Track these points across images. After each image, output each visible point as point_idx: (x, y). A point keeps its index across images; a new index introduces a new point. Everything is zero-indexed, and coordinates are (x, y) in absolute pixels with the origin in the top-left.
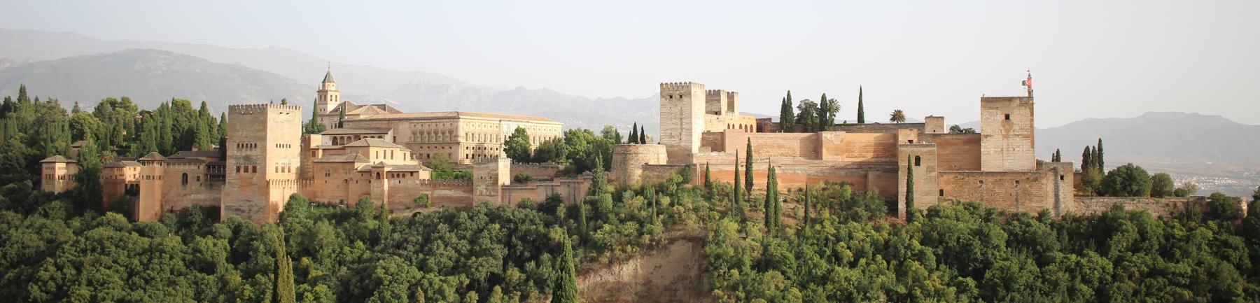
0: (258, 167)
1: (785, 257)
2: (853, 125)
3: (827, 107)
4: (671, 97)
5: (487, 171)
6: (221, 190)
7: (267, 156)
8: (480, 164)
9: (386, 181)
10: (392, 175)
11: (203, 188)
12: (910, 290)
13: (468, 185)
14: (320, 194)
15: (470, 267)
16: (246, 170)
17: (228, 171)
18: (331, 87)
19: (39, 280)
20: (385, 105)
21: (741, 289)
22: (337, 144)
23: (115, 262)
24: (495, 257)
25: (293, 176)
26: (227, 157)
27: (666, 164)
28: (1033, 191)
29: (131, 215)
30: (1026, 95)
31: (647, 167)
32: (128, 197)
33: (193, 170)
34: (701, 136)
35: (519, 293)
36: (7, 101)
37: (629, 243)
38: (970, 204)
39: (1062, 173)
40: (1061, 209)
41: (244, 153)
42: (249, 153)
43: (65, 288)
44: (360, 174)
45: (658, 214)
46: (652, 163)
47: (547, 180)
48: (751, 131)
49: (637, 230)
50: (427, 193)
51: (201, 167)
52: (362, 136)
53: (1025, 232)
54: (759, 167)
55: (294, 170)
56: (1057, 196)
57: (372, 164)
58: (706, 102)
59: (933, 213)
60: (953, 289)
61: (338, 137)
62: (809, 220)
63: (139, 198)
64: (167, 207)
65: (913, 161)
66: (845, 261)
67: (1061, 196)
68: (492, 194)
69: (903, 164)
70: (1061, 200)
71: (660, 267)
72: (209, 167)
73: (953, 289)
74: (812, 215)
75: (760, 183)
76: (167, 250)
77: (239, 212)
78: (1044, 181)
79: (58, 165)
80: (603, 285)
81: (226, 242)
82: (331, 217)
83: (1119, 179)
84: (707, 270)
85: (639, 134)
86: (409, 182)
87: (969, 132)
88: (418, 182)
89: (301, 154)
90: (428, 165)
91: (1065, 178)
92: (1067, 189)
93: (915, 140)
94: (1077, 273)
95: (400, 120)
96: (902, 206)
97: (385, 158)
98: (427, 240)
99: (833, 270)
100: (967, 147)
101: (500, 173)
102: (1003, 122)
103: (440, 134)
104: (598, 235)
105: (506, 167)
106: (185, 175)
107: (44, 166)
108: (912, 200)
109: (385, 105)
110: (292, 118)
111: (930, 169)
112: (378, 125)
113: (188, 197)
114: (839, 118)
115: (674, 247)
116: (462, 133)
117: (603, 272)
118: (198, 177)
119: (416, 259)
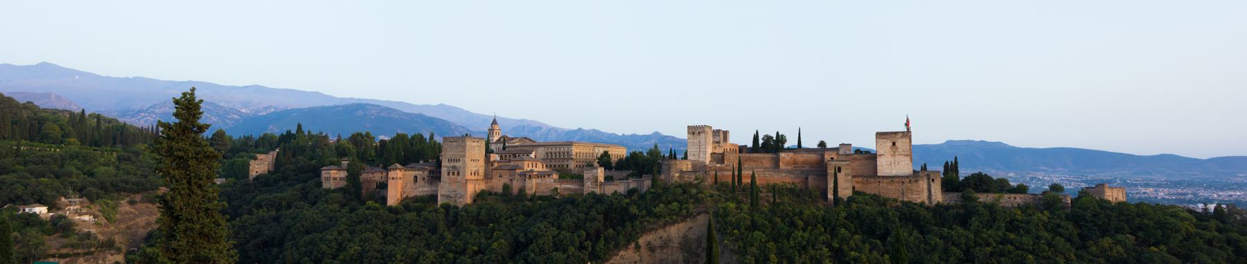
3: (781, 139)
5: (591, 174)
16: (453, 174)
29: (384, 199)
30: (906, 130)
32: (378, 190)
35: (614, 242)
38: (874, 195)
40: (933, 199)
41: (452, 164)
42: (455, 164)
45: (690, 198)
46: (684, 170)
52: (517, 155)
53: (910, 214)
54: (746, 173)
58: (713, 136)
60: (867, 245)
61: (504, 155)
63: (387, 190)
64: (405, 196)
67: (933, 191)
69: (831, 171)
70: (933, 194)
71: (691, 228)
72: (430, 173)
75: (746, 181)
78: (921, 182)
80: (661, 238)
88: (552, 180)
93: (835, 158)
95: (539, 146)
96: (830, 196)
98: (560, 213)
99: (793, 232)
104: (657, 210)
106: (416, 177)
111: (847, 175)
112: (527, 148)
114: (786, 146)
115: (699, 217)
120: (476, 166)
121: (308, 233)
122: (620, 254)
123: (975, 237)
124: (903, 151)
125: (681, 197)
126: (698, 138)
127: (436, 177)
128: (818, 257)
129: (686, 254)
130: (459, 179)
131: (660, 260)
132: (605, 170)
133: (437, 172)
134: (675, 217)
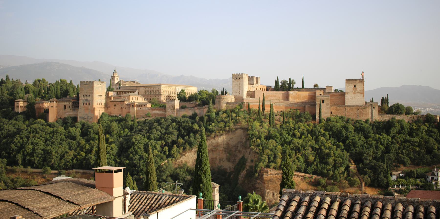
0: (91, 103)
1: (276, 135)
2: (300, 89)
3: (291, 82)
4: (236, 79)
5: (171, 104)
6: (77, 111)
7: (94, 99)
8: (168, 102)
9: (136, 108)
10: (138, 106)
11: (71, 110)
12: (320, 146)
13: (164, 109)
14: (112, 113)
15: (165, 138)
16: (86, 104)
17: (80, 105)
18: (116, 75)
19: (14, 142)
20: (135, 81)
21: (260, 146)
22: (118, 95)
23: (41, 136)
24: (174, 135)
25: (103, 106)
26: (80, 100)
27: (234, 102)
28: (364, 112)
29: (46, 120)
30: (362, 78)
31: (227, 103)
32: (45, 114)
33: (68, 104)
34: (246, 92)
35: (183, 147)
36: (2, 80)
37: (221, 130)
38: (341, 117)
39: (374, 106)
40: (373, 119)
41: (86, 98)
42: (87, 98)
43: (23, 145)
44: (126, 106)
45: (231, 120)
46: (229, 102)
47: (192, 108)
48: (264, 91)
49: (224, 125)
50: (150, 112)
51: (71, 103)
52: (127, 92)
53: (361, 127)
54: (267, 103)
55: (103, 104)
56: (372, 114)
57: (130, 102)
58: (249, 80)
59: (328, 120)
60: (335, 147)
61: (119, 92)
62: (285, 122)
63: (49, 114)
64: (59, 117)
65: (321, 101)
66: (297, 136)
67: (374, 114)
68: (173, 112)
69: (318, 103)
70: (374, 115)
71: (232, 138)
72: (73, 103)
73: (335, 147)
74: (286, 120)
75: (267, 109)
76: (59, 132)
77: (84, 119)
78: (368, 109)
79: (20, 103)
81: (80, 129)
82: (116, 121)
83: (394, 109)
84: (248, 139)
85: (225, 92)
86: (144, 108)
87: (341, 91)
88: (147, 108)
89: (106, 98)
90: (150, 102)
91: (375, 108)
92: (376, 112)
93: (322, 95)
94: (379, 141)
95: (140, 86)
96: (317, 117)
97: (135, 100)
98: (150, 129)
99: (293, 140)
100: (340, 97)
101: (176, 105)
102: (353, 88)
103: (154, 92)
104: (210, 127)
105: (178, 103)
106: (65, 106)
107: (15, 103)
108: (321, 115)
109: (135, 81)
110: (102, 86)
111: (327, 105)
113: (66, 113)
114: (295, 86)
115: (236, 131)
116: (162, 91)
117: (212, 140)
118: (70, 107)
119: (146, 135)
120: (100, 100)
121: (5, 137)
122: (187, 155)
123: (392, 139)
124: (360, 91)
125: (226, 119)
126: (239, 81)
127: (77, 106)
128: (306, 154)
129: (228, 155)
130: (90, 107)
131: (212, 158)
132: (180, 102)
133: (77, 103)
134: (221, 131)
